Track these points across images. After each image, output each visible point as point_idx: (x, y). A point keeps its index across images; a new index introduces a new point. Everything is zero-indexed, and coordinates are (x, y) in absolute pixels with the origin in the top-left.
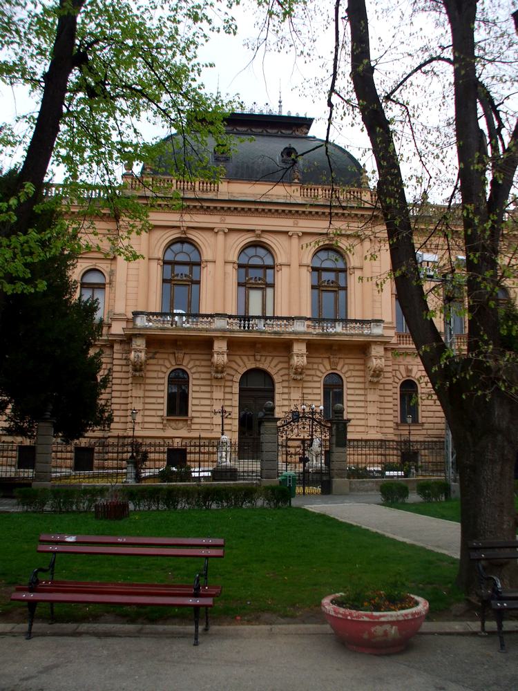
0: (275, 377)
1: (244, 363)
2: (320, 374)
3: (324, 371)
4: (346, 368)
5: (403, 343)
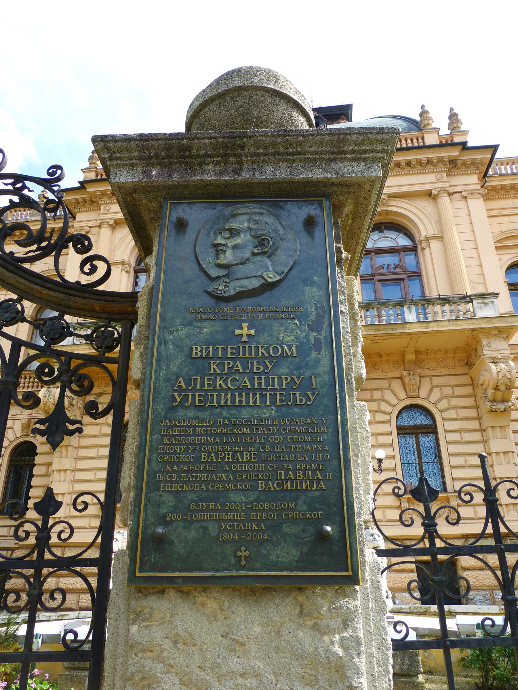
2: (388, 409)
3: (394, 401)
4: (436, 391)
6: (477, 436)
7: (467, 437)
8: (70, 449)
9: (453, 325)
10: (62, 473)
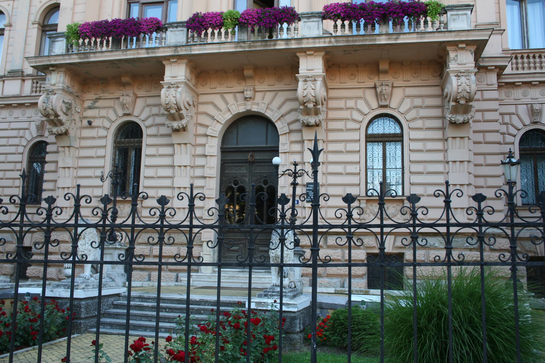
0: (278, 125)
1: (227, 103)
2: (359, 117)
3: (366, 110)
5: (523, 68)
6: (439, 145)
7: (430, 145)
8: (72, 149)
9: (421, 38)
10: (67, 169)
